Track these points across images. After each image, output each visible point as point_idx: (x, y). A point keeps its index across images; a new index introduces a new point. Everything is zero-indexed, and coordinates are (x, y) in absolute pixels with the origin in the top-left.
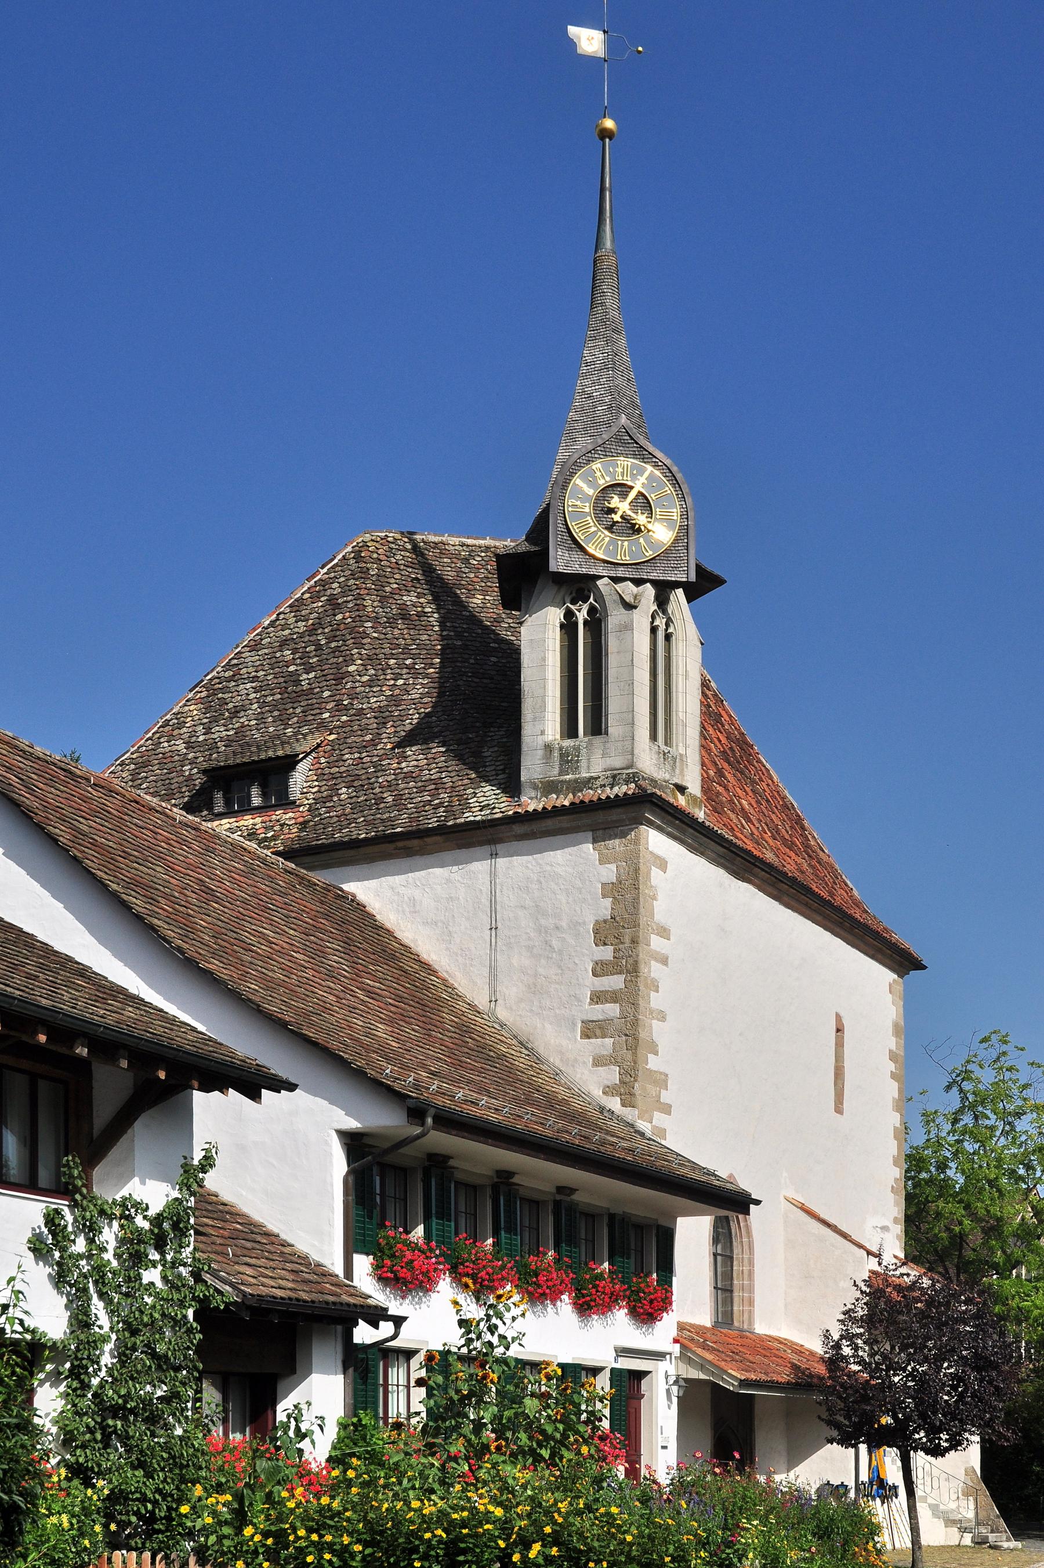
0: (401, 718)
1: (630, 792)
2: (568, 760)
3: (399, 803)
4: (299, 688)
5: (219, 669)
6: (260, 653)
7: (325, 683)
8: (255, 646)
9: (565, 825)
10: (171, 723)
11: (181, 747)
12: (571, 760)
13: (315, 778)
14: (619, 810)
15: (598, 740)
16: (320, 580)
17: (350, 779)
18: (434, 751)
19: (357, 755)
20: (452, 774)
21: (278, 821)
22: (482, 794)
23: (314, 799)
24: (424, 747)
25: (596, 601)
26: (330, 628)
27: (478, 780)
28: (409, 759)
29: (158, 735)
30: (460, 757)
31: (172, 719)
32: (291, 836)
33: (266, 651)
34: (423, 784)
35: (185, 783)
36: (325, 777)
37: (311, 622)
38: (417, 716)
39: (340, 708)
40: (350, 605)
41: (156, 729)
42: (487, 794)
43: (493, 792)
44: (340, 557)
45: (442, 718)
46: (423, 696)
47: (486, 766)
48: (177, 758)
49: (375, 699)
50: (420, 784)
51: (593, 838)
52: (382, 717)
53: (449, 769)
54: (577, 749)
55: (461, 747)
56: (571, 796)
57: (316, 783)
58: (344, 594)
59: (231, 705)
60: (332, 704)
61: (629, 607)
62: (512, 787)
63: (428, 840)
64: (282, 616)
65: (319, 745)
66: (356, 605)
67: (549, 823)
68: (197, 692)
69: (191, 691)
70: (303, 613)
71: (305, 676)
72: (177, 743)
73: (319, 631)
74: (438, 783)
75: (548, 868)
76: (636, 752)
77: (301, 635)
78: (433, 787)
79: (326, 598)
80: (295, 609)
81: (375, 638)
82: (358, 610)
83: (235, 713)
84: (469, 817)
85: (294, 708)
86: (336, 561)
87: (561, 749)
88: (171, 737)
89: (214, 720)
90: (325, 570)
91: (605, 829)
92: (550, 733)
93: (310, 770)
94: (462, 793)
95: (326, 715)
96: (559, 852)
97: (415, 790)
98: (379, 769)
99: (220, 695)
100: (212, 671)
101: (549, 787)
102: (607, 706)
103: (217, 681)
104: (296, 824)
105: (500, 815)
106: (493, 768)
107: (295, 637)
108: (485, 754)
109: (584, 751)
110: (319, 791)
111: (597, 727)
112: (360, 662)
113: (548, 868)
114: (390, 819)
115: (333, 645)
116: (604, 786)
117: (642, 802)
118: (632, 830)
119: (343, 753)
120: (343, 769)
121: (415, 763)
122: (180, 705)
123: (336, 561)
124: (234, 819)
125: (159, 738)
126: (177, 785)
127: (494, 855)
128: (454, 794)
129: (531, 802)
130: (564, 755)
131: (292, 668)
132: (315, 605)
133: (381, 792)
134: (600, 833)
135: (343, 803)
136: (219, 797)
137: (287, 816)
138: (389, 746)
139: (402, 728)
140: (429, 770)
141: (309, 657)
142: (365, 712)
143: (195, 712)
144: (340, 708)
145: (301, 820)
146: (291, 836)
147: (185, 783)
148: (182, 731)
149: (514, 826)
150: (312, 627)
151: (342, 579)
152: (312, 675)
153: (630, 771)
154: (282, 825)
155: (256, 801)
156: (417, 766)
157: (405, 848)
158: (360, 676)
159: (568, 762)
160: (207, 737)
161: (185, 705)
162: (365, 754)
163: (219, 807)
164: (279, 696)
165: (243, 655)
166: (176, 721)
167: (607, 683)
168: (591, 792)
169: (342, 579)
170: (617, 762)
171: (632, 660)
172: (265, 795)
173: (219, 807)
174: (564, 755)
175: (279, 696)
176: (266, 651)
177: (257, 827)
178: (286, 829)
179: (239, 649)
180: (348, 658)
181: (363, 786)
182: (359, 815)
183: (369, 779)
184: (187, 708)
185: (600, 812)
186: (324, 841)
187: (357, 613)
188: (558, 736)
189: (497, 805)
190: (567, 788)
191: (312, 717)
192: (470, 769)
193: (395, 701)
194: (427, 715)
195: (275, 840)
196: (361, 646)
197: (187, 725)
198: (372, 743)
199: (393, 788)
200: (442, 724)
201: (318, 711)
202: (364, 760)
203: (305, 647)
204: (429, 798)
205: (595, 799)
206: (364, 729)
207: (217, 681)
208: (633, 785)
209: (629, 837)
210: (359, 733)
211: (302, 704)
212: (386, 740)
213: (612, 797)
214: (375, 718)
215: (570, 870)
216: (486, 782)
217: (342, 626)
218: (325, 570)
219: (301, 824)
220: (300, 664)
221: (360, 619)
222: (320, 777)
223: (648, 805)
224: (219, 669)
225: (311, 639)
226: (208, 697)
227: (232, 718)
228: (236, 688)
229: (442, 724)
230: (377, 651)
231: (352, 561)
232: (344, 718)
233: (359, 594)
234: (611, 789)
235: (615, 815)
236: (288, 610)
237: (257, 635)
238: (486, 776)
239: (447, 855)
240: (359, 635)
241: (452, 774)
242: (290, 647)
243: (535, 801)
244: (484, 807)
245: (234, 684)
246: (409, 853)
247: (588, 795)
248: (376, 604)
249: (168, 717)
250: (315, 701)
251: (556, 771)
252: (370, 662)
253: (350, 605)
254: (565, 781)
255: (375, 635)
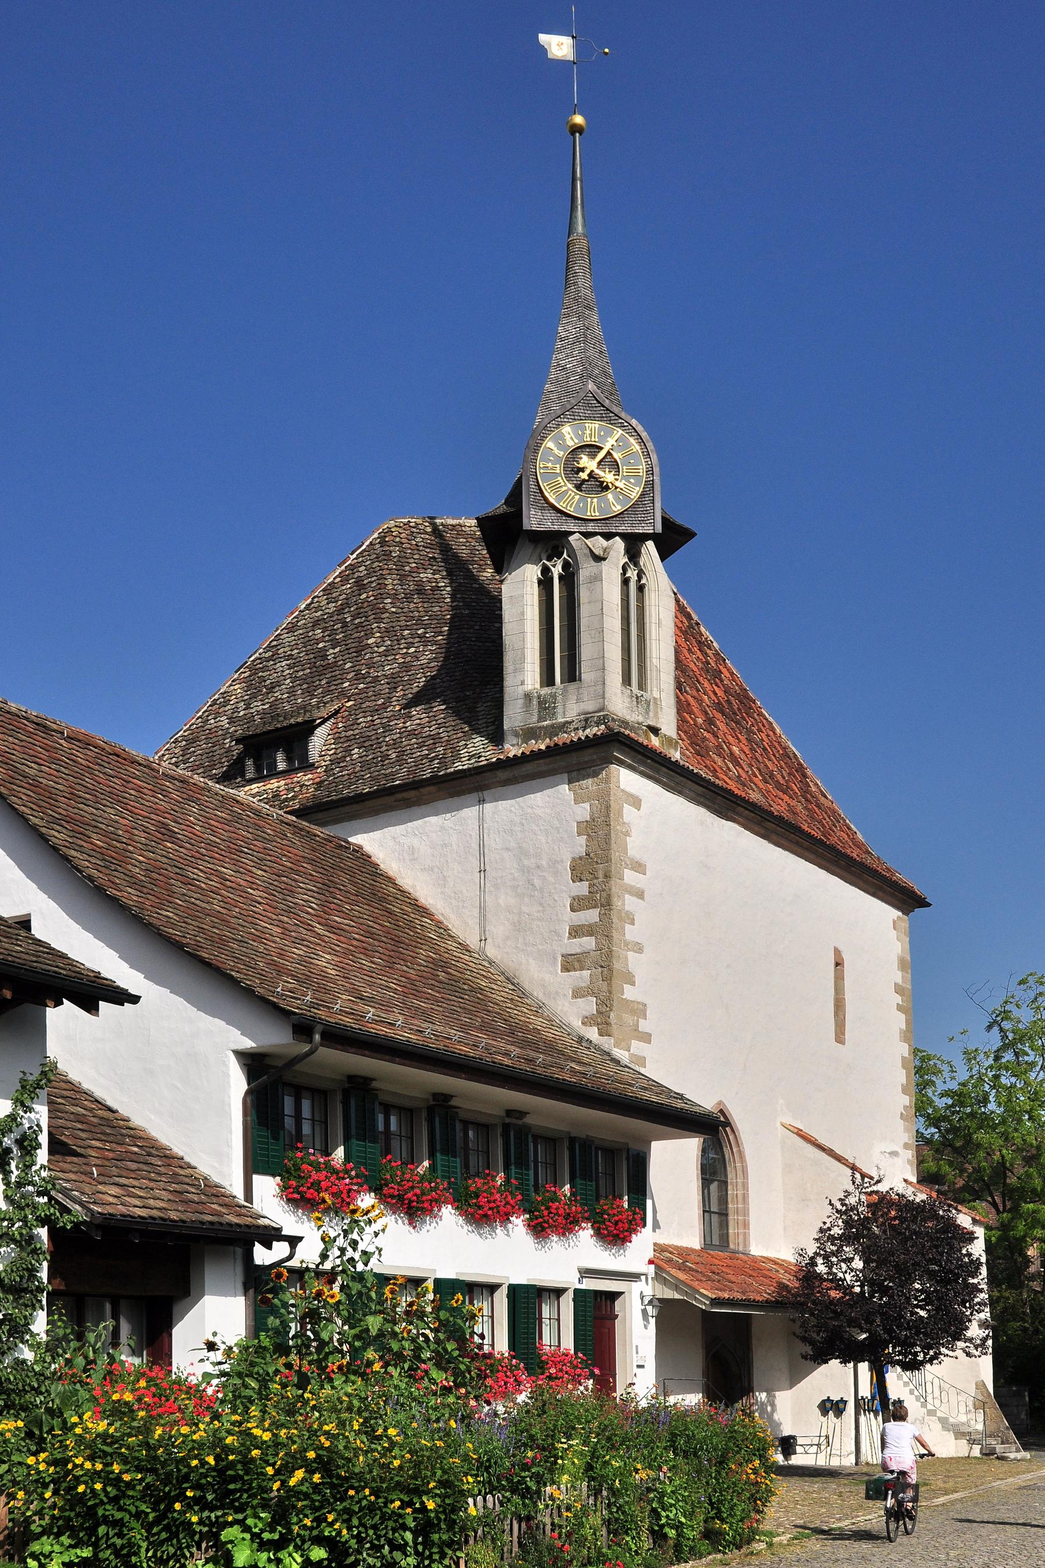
0: (410, 682)
1: (599, 733)
2: (546, 707)
3: (400, 760)
4: (326, 662)
5: (261, 651)
6: (295, 634)
7: (347, 656)
8: (291, 628)
9: (544, 768)
10: (218, 702)
11: (224, 722)
12: (549, 707)
13: (333, 741)
14: (591, 751)
15: (572, 687)
16: (350, 565)
17: (362, 740)
18: (435, 709)
19: (369, 718)
20: (449, 729)
21: (298, 782)
22: (472, 745)
23: (330, 760)
24: (428, 706)
25: (569, 556)
26: (355, 607)
27: (470, 732)
28: (413, 719)
29: (207, 713)
30: (457, 714)
31: (219, 699)
32: (308, 795)
33: (301, 632)
34: (423, 740)
35: (225, 755)
36: (342, 740)
37: (340, 602)
38: (424, 679)
39: (359, 677)
40: (374, 585)
41: (205, 708)
42: (476, 745)
43: (481, 743)
44: (367, 543)
45: (445, 679)
46: (431, 660)
47: (478, 720)
48: (220, 732)
49: (389, 667)
50: (420, 740)
51: (569, 780)
52: (394, 682)
53: (447, 725)
54: (554, 696)
55: (458, 704)
56: (548, 740)
57: (333, 746)
58: (368, 575)
59: (268, 682)
60: (353, 674)
61: (598, 559)
62: (497, 737)
63: (424, 790)
64: (316, 600)
65: (337, 712)
66: (379, 584)
67: (529, 768)
68: (242, 673)
69: (236, 672)
70: (334, 595)
71: (331, 651)
72: (222, 719)
73: (346, 611)
74: (436, 738)
75: (529, 810)
76: (607, 695)
77: (331, 615)
78: (432, 741)
79: (353, 580)
80: (327, 592)
81: (393, 612)
82: (379, 589)
83: (271, 689)
84: (459, 766)
85: (320, 680)
86: (364, 547)
87: (539, 697)
88: (217, 714)
89: (253, 697)
90: (354, 556)
91: (579, 770)
92: (529, 683)
93: (329, 735)
94: (455, 745)
95: (346, 684)
96: (539, 794)
97: (415, 746)
98: (388, 729)
99: (260, 674)
100: (255, 653)
101: (530, 734)
102: (580, 654)
103: (259, 661)
104: (313, 784)
105: (485, 762)
106: (485, 720)
107: (325, 617)
108: (478, 709)
109: (559, 698)
110: (335, 753)
111: (572, 674)
112: (378, 635)
113: (529, 810)
114: (392, 774)
115: (357, 621)
116: (577, 729)
117: (610, 741)
118: (603, 769)
119: (358, 717)
120: (357, 731)
121: (418, 721)
122: (227, 685)
123: (364, 547)
124: (262, 784)
125: (207, 716)
126: (218, 757)
127: (482, 801)
128: (449, 747)
129: (512, 749)
130: (542, 702)
131: (321, 645)
132: (344, 587)
133: (387, 750)
134: (574, 774)
135: (354, 762)
136: (249, 763)
137: (307, 778)
138: (398, 708)
139: (410, 691)
140: (430, 727)
141: (336, 634)
142: (379, 679)
143: (239, 691)
144: (359, 677)
145: (318, 780)
146: (308, 795)
147: (225, 755)
148: (226, 709)
149: (498, 772)
150: (340, 607)
151: (368, 562)
152: (337, 650)
153: (602, 714)
154: (301, 786)
155: (281, 766)
156: (420, 724)
157: (404, 799)
158: (378, 647)
159: (546, 708)
160: (247, 711)
161: (231, 685)
162: (376, 717)
163: (250, 773)
164: (309, 671)
165: (282, 637)
166: (222, 700)
167: (579, 633)
168: (566, 735)
169: (368, 562)
170: (590, 706)
171: (602, 609)
172: (289, 760)
173: (250, 773)
174: (542, 702)
175: (309, 671)
176: (301, 632)
177: (281, 789)
178: (304, 788)
179: (279, 631)
180: (368, 632)
181: (372, 745)
182: (367, 771)
183: (378, 739)
184: (232, 688)
185: (573, 754)
186: (334, 797)
187: (379, 591)
188: (538, 686)
189: (483, 754)
190: (545, 733)
191: (334, 687)
192: (465, 723)
193: (406, 667)
194: (433, 678)
195: (294, 800)
196: (380, 620)
197: (232, 703)
198: (383, 706)
199: (397, 745)
200: (445, 684)
201: (340, 681)
202: (375, 723)
203: (334, 626)
204: (427, 752)
205: (568, 741)
206: (377, 695)
207: (259, 661)
208: (603, 727)
209: (600, 776)
210: (373, 698)
211: (327, 676)
212: (395, 703)
213: (583, 738)
214: (388, 683)
215: (548, 811)
216: (477, 734)
217: (366, 604)
218: (354, 556)
219: (317, 783)
220: (328, 641)
221: (380, 597)
222: (337, 740)
223: (617, 745)
224: (261, 651)
225: (339, 617)
226: (250, 676)
227: (268, 693)
228: (273, 667)
229: (445, 684)
230: (394, 624)
231: (378, 546)
232: (362, 686)
233: (381, 574)
234: (583, 731)
235: (587, 755)
236: (321, 593)
237: (295, 618)
238: (478, 729)
239: (440, 804)
240: (378, 611)
241: (449, 729)
242: (321, 627)
243: (516, 747)
244: (472, 756)
245: (272, 663)
246: (408, 804)
247: (563, 738)
248: (395, 582)
249: (216, 697)
250: (338, 672)
251: (535, 718)
252: (387, 634)
253: (374, 585)
254: (543, 727)
255: (394, 610)
